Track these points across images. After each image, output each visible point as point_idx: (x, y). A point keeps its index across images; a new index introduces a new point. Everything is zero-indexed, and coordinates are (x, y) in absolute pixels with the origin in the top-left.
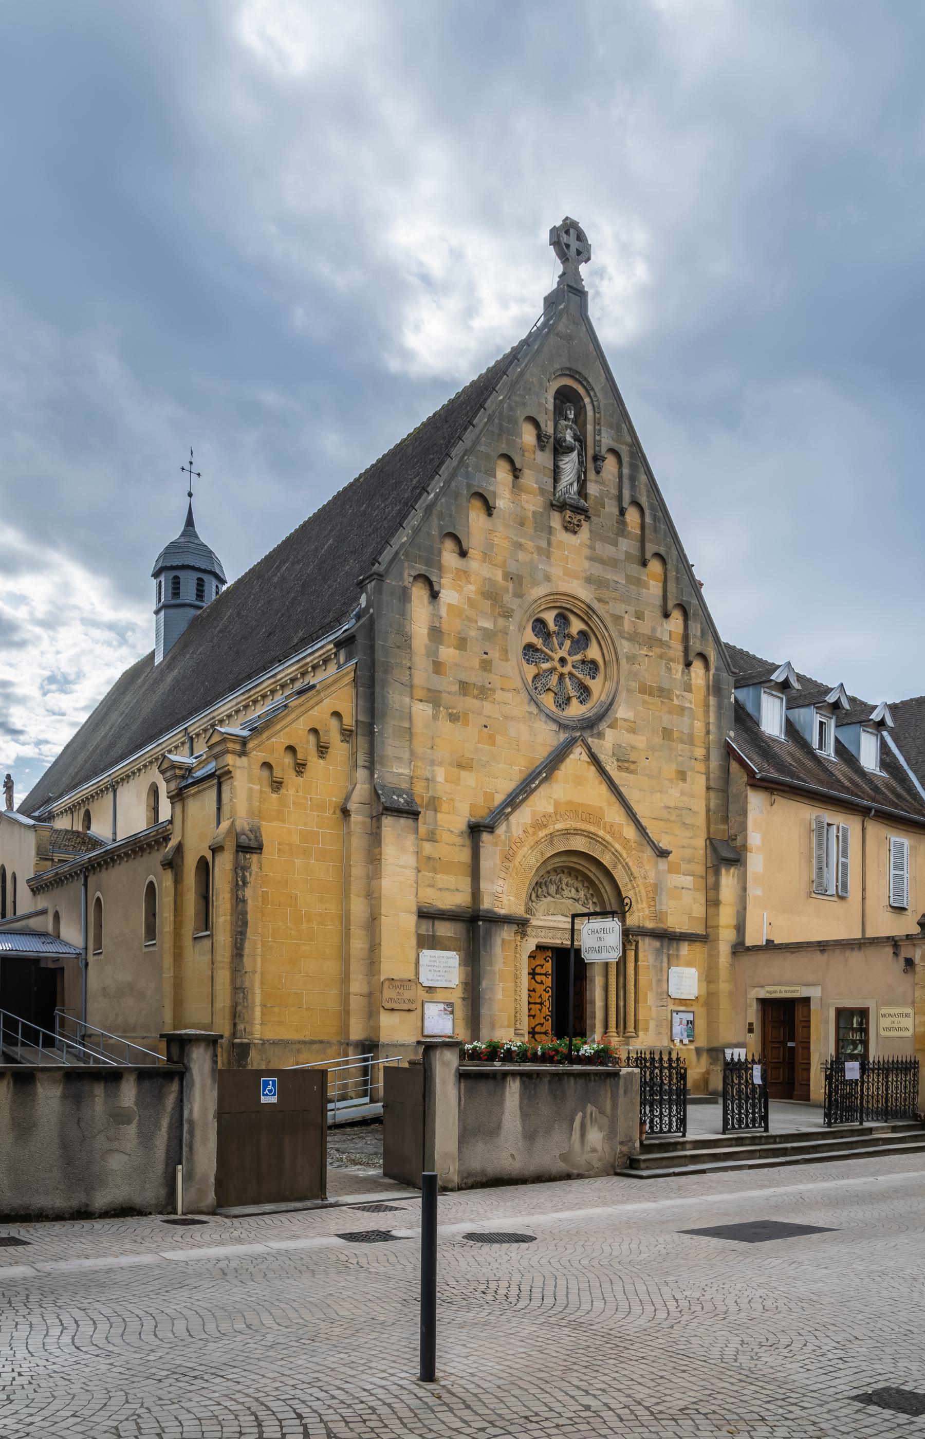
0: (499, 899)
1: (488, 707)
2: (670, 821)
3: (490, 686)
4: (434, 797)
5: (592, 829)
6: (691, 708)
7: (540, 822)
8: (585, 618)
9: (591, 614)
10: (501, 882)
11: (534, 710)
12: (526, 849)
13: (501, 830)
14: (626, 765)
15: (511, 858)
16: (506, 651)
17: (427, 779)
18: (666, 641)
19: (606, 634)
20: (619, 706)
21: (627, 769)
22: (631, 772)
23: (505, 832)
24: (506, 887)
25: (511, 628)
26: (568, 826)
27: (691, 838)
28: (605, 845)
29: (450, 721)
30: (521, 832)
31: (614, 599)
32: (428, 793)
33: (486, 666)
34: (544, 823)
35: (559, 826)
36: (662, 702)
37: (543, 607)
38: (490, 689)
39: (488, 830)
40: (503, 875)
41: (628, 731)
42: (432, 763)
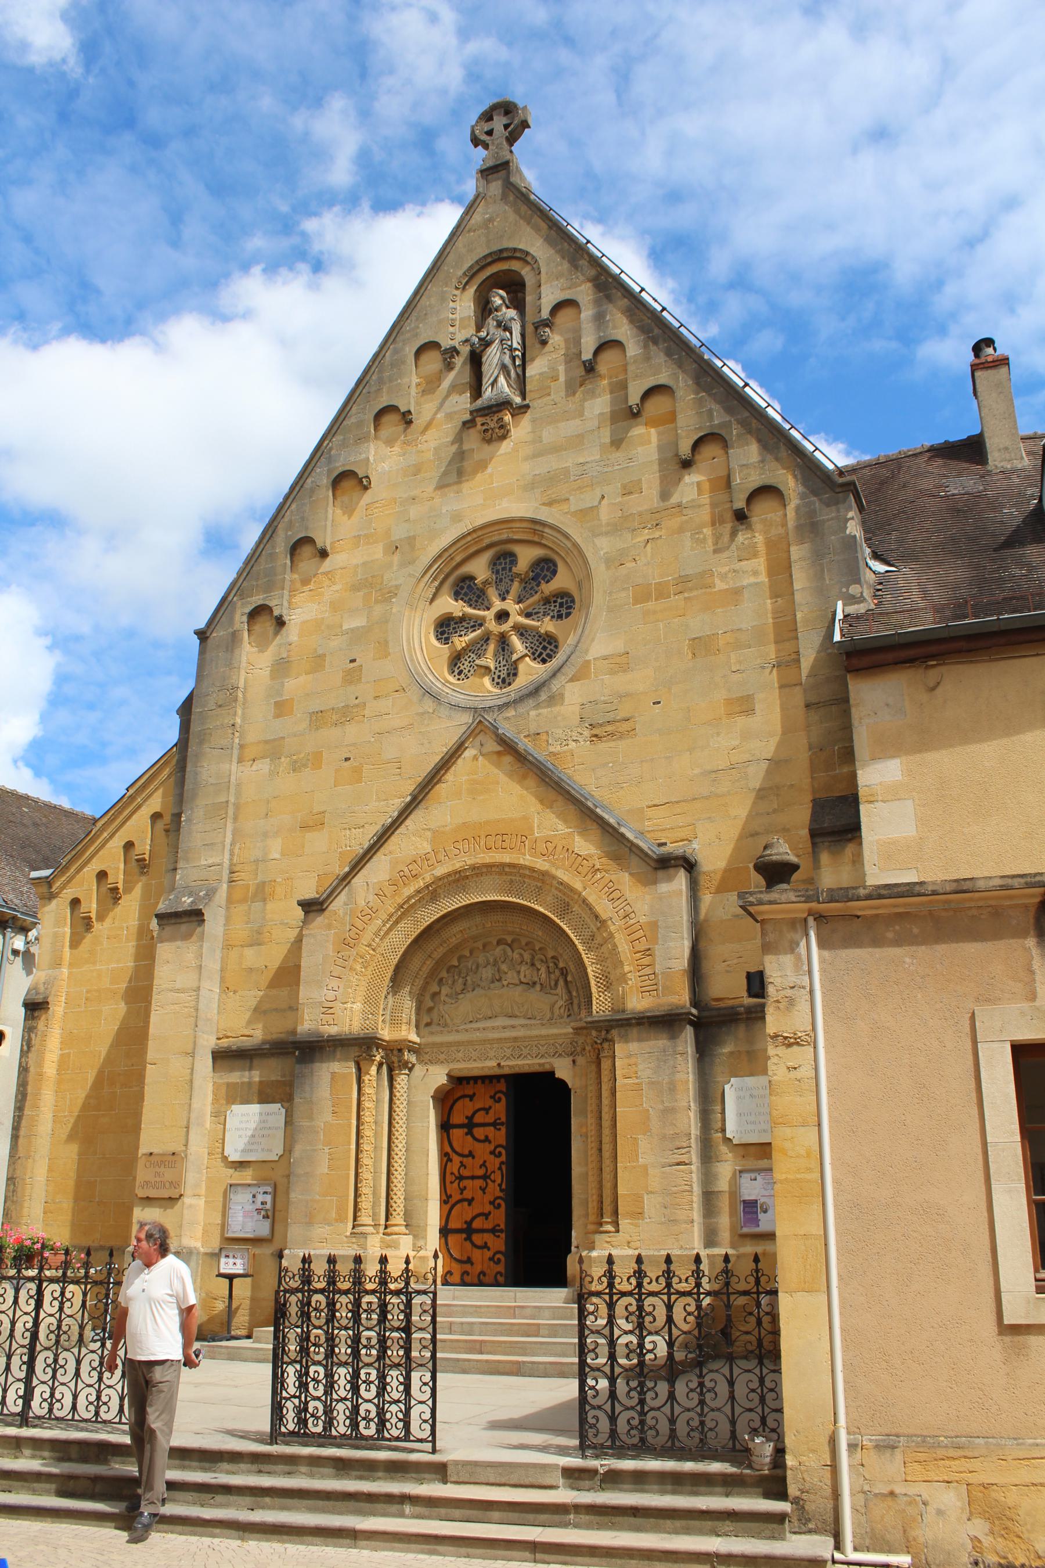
0: (331, 1011)
1: (352, 732)
3: (357, 702)
4: (264, 883)
5: (506, 858)
6: (756, 584)
8: (536, 539)
9: (541, 529)
10: (334, 983)
11: (429, 705)
12: (379, 922)
13: (338, 904)
14: (610, 728)
16: (386, 642)
17: (257, 861)
18: (693, 500)
19: (569, 545)
20: (593, 640)
21: (613, 734)
22: (622, 736)
23: (346, 904)
24: (341, 990)
25: (394, 610)
26: (458, 866)
27: (775, 811)
28: (541, 880)
30: (371, 897)
31: (580, 488)
32: (256, 879)
33: (353, 674)
35: (440, 871)
36: (685, 598)
37: (458, 559)
38: (357, 706)
39: (315, 908)
41: (612, 672)
42: (266, 835)
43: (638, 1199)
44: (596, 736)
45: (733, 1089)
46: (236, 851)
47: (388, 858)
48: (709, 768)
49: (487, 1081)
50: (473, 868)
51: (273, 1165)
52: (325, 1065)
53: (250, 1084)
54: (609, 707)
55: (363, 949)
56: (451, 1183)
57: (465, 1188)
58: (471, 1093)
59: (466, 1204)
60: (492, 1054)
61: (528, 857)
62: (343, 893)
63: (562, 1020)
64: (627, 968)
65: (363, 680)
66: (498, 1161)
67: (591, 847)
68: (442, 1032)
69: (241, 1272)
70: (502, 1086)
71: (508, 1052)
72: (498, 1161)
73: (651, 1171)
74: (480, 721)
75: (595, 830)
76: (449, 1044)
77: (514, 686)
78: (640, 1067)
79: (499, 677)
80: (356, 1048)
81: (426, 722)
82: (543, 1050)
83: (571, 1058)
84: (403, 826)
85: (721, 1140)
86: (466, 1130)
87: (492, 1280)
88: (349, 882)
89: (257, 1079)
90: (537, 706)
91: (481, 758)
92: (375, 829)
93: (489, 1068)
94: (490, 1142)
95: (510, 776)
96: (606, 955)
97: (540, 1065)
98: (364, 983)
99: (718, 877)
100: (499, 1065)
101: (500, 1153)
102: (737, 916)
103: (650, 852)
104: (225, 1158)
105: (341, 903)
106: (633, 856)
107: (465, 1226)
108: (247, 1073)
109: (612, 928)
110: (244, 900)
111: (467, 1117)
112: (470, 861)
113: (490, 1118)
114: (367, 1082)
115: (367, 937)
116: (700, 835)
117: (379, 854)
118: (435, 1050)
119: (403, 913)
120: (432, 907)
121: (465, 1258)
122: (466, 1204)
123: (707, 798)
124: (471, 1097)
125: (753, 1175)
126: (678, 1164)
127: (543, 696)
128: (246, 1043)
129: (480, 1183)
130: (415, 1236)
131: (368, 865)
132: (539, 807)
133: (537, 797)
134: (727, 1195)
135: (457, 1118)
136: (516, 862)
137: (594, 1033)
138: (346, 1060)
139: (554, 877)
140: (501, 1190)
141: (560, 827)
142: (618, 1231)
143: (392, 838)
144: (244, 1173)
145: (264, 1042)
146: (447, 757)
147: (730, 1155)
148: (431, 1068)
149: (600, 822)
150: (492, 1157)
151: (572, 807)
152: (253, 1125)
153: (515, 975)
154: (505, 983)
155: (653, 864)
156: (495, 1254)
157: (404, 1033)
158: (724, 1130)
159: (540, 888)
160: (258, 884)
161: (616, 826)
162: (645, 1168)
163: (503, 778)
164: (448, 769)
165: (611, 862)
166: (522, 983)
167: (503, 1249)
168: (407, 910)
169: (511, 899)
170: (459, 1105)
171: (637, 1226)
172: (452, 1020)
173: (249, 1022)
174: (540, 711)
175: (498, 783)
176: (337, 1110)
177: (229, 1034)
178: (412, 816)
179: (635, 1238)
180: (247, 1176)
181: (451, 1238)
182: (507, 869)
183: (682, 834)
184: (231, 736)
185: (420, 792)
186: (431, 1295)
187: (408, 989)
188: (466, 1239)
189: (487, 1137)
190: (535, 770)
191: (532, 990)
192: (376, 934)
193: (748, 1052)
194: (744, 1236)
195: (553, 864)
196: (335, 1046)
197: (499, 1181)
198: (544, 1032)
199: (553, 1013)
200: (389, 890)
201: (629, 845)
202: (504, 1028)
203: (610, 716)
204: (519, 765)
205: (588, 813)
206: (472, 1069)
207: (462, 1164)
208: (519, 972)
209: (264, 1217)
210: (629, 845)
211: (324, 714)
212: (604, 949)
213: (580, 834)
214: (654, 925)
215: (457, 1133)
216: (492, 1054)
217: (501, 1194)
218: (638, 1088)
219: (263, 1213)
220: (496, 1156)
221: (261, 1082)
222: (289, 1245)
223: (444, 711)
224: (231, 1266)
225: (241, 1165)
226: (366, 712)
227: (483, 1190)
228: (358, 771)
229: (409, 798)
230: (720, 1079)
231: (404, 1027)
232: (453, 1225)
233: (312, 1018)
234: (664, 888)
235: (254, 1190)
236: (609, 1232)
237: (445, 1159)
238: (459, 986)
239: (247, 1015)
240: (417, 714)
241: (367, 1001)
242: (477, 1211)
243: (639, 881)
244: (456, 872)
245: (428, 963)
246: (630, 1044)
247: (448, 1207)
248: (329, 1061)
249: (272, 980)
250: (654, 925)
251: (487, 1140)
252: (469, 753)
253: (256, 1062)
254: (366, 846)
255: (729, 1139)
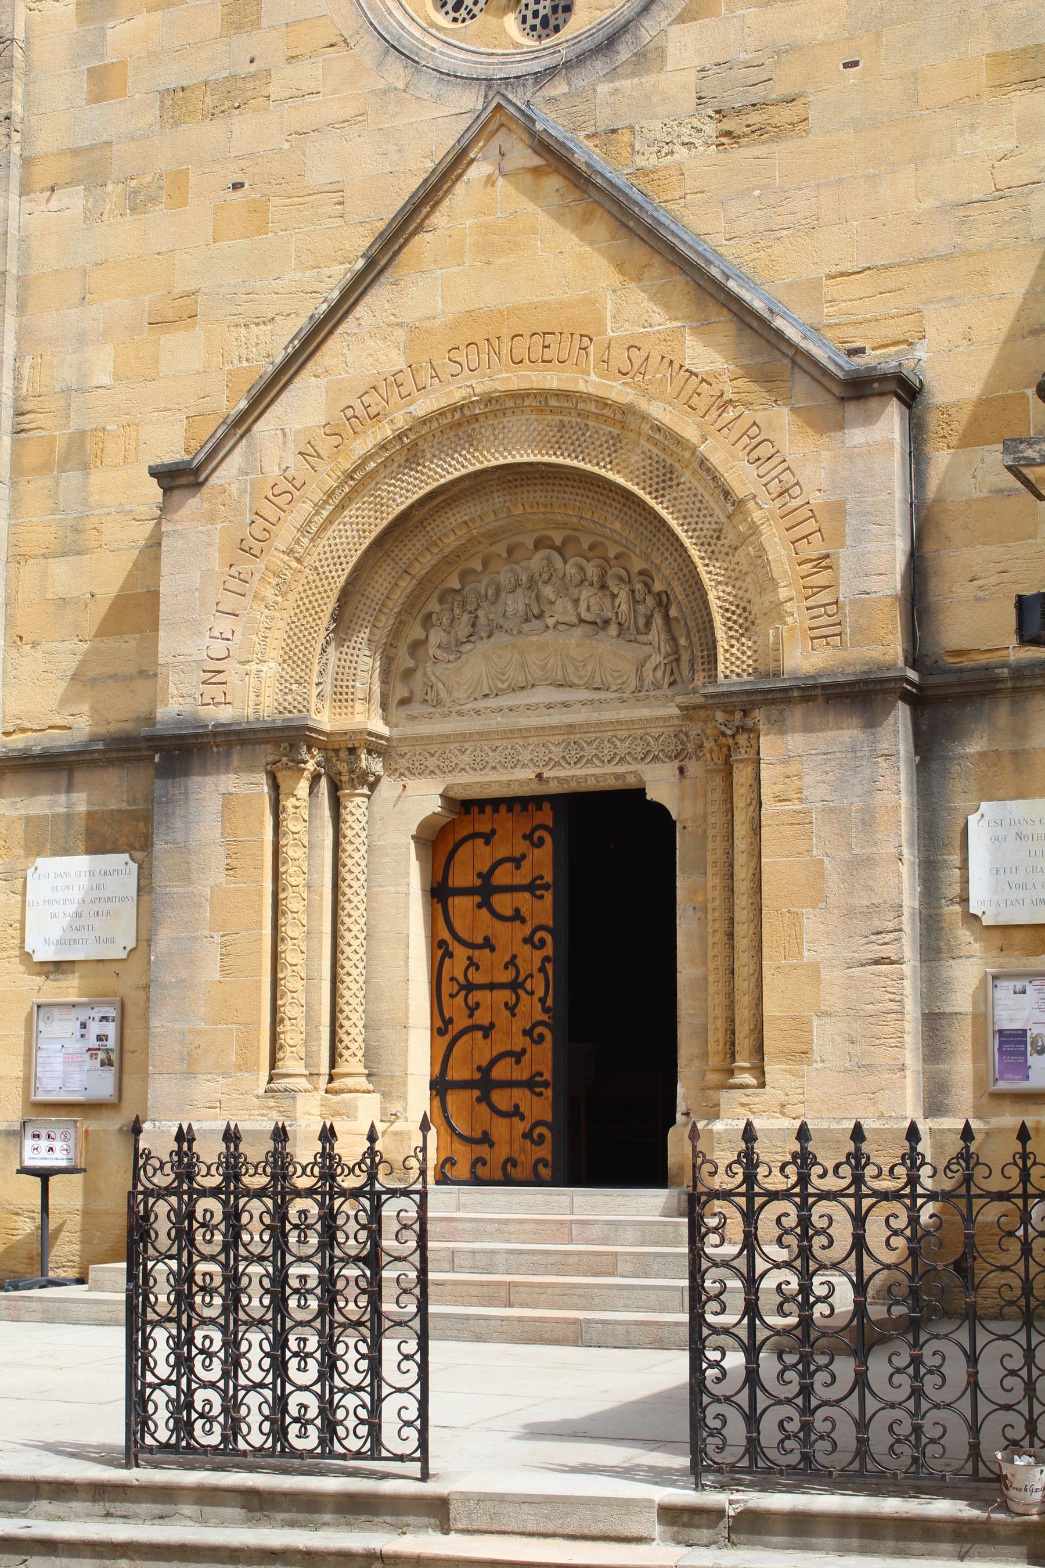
0: (219, 678)
2: (968, 254)
3: (253, 68)
4: (82, 433)
5: (552, 380)
7: (360, 411)
10: (225, 625)
11: (396, 73)
12: (308, 507)
14: (755, 118)
15: (257, 546)
17: (66, 391)
21: (761, 131)
22: (780, 133)
26: (458, 395)
29: (133, 210)
30: (292, 459)
32: (66, 425)
34: (372, 411)
35: (423, 406)
38: (254, 76)
39: (184, 481)
40: (230, 602)
42: (82, 339)
43: (801, 1025)
44: (728, 134)
45: (984, 822)
46: (26, 372)
47: (323, 381)
48: (952, 197)
49: (517, 808)
50: (488, 399)
51: (117, 967)
52: (210, 780)
53: (69, 818)
54: (754, 75)
55: (277, 559)
56: (452, 996)
57: (478, 1005)
58: (486, 829)
59: (479, 1034)
60: (526, 756)
61: (593, 377)
62: (238, 450)
63: (658, 693)
64: (783, 593)
65: (264, 23)
66: (538, 955)
67: (717, 357)
68: (430, 716)
69: (64, 1164)
70: (546, 816)
71: (557, 752)
72: (538, 955)
73: (824, 973)
74: (499, 106)
75: (725, 326)
76: (446, 739)
77: (566, 33)
78: (808, 780)
79: (536, 14)
80: (270, 748)
81: (391, 109)
82: (622, 748)
83: (676, 764)
84: (350, 318)
85: (959, 918)
86: (478, 899)
87: (526, 1173)
88: (248, 430)
89: (83, 808)
90: (612, 74)
91: (500, 182)
92: (298, 323)
93: (521, 783)
94: (523, 921)
95: (559, 217)
96: (745, 568)
97: (617, 776)
98: (281, 624)
99: (964, 416)
100: (539, 776)
101: (542, 942)
102: (999, 491)
103: (831, 367)
104: (26, 957)
105: (234, 471)
106: (799, 375)
107: (477, 1076)
108: (63, 798)
109: (757, 515)
110: (44, 468)
111: (480, 875)
112: (482, 386)
113: (523, 877)
114: (290, 810)
115: (285, 535)
116: (930, 332)
117: (304, 374)
118: (418, 749)
119: (353, 490)
120: (409, 477)
121: (478, 1134)
122: (479, 1034)
123: (945, 258)
124: (488, 838)
125: (1019, 984)
126: (877, 962)
127: (624, 52)
128: (60, 741)
129: (506, 995)
130: (385, 1095)
131: (283, 397)
132: (616, 278)
133: (611, 259)
134: (969, 1020)
135: (462, 876)
136: (571, 387)
137: (720, 716)
138: (251, 769)
139: (644, 417)
140: (546, 1010)
141: (656, 318)
142: (762, 1085)
143: (330, 343)
144: (64, 984)
145: (93, 740)
146: (433, 180)
147: (976, 946)
148: (413, 784)
149: (735, 308)
150: (528, 948)
151: (679, 278)
152: (78, 895)
153: (570, 606)
154: (551, 622)
155: (837, 390)
156: (534, 1126)
157: (358, 718)
158: (965, 900)
159: (618, 439)
160: (71, 438)
161: (766, 315)
162: (815, 969)
163: (544, 220)
164: (437, 203)
165: (755, 387)
166: (582, 621)
167: (548, 1117)
168: (362, 483)
169: (561, 460)
170: (464, 852)
171: (797, 1075)
172: (449, 692)
173: (65, 701)
174: (618, 84)
175: (534, 231)
176: (234, 863)
177: (26, 724)
178: (368, 299)
179: (794, 1098)
180: (69, 989)
181: (453, 1099)
182: (553, 402)
183: (894, 332)
184: (5, 140)
185: (383, 250)
186: (417, 1197)
187: (365, 633)
188: (479, 1100)
189: (517, 911)
190: (608, 204)
191: (602, 635)
192: (303, 530)
193: (1015, 754)
194: (999, 1096)
195: (644, 392)
196: (229, 745)
197: (540, 992)
198: (625, 714)
199: (641, 679)
200: (325, 445)
201: (790, 352)
202: (549, 706)
203: (757, 94)
204: (577, 194)
205: (712, 290)
206: (489, 784)
207: (472, 963)
208: (576, 602)
209: (103, 1064)
210: (790, 352)
211: (188, 94)
212: (740, 555)
213: (696, 331)
214: (838, 510)
215: (461, 905)
216: (526, 756)
217: (545, 1017)
218: (803, 819)
219: (101, 1055)
220: (534, 946)
221: (90, 814)
222: (151, 1114)
223: (427, 86)
224: (44, 1153)
225: (58, 968)
226: (273, 90)
227: (511, 1009)
228: (258, 211)
229: (360, 264)
230: (959, 803)
231: (359, 707)
232: (453, 1074)
233: (184, 691)
234: (857, 436)
235: (83, 1014)
236: (746, 1087)
237: (440, 952)
238: (462, 628)
239: (61, 687)
240: (373, 92)
241: (288, 658)
242: (499, 1048)
243: (810, 424)
244: (455, 408)
245: (403, 584)
246: (789, 737)
247: (447, 1038)
248: (218, 772)
249: (105, 620)
250: (838, 510)
251: (517, 916)
252: (478, 172)
253: (79, 777)
254: (279, 359)
255: (975, 916)
